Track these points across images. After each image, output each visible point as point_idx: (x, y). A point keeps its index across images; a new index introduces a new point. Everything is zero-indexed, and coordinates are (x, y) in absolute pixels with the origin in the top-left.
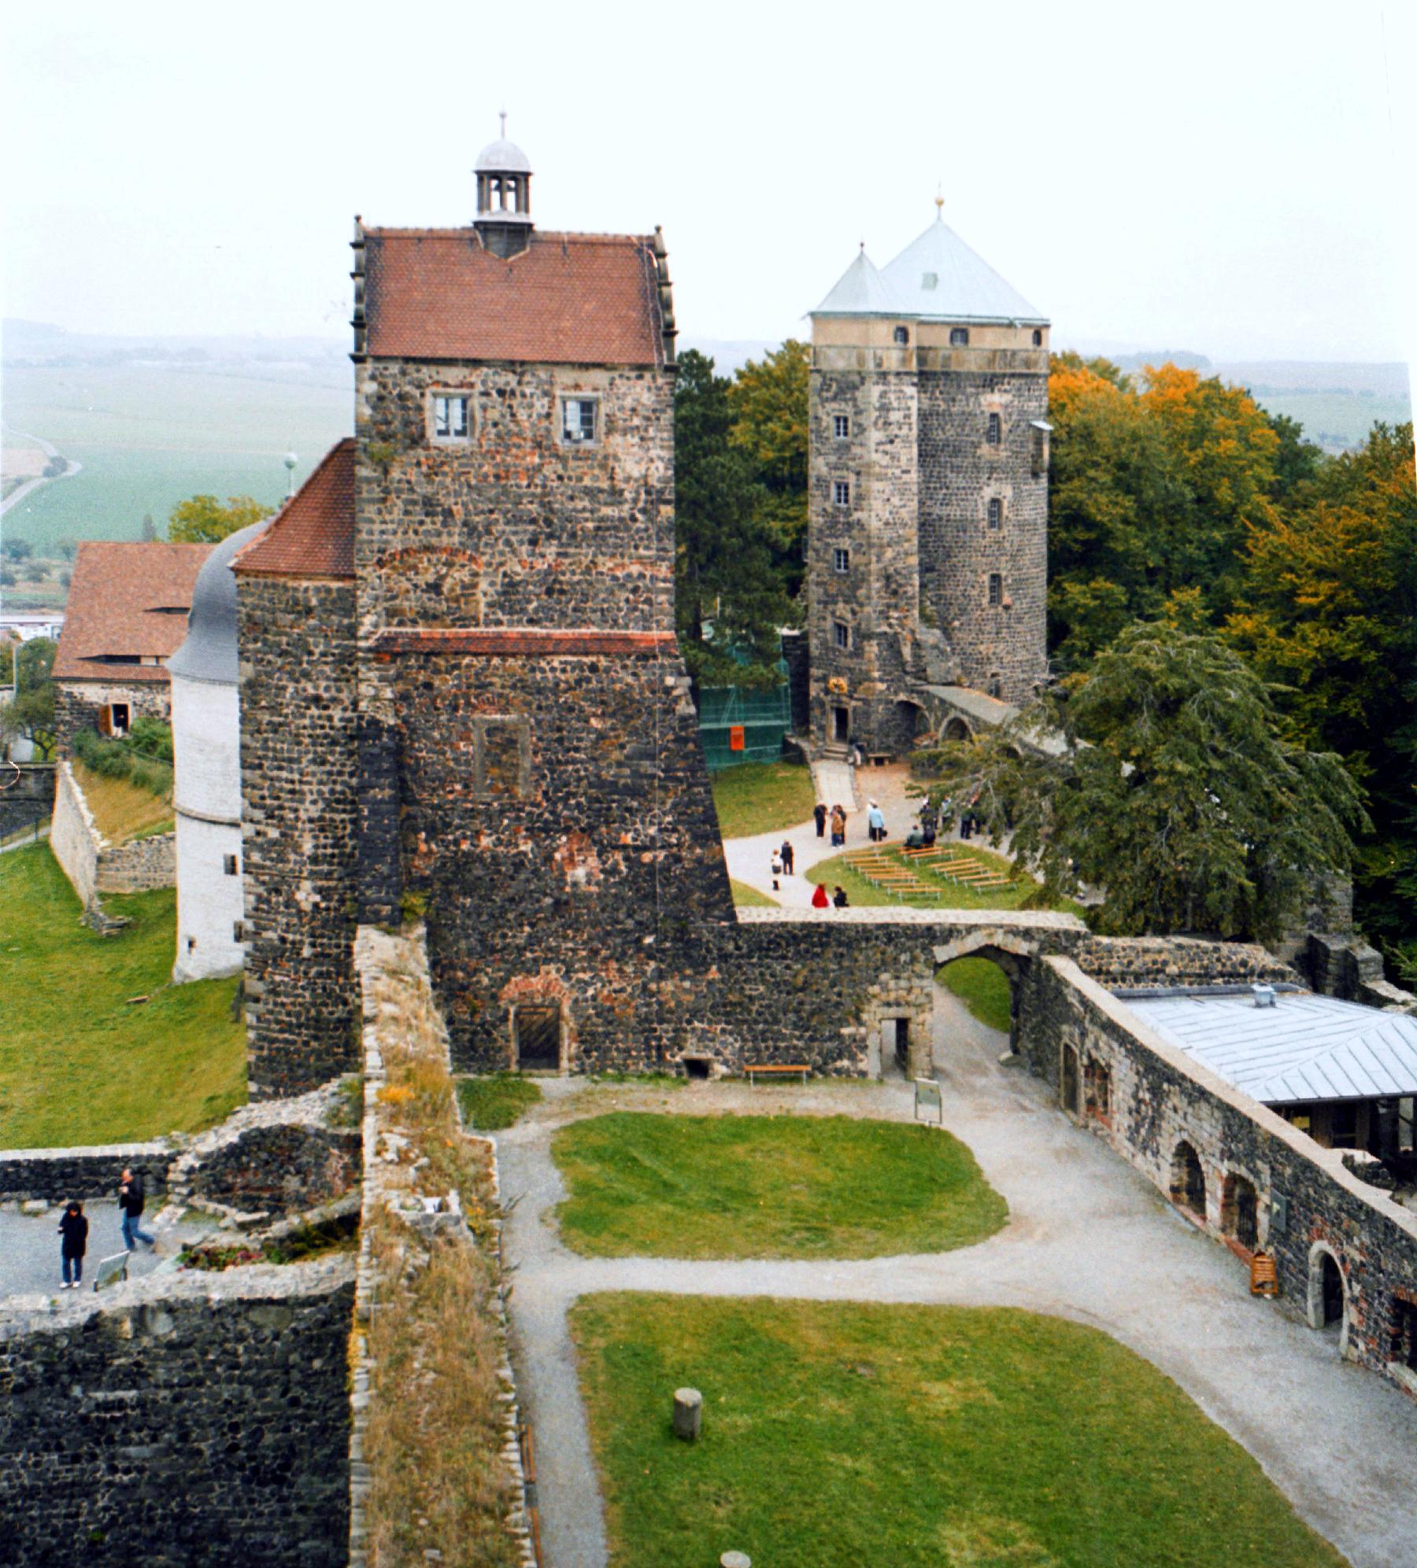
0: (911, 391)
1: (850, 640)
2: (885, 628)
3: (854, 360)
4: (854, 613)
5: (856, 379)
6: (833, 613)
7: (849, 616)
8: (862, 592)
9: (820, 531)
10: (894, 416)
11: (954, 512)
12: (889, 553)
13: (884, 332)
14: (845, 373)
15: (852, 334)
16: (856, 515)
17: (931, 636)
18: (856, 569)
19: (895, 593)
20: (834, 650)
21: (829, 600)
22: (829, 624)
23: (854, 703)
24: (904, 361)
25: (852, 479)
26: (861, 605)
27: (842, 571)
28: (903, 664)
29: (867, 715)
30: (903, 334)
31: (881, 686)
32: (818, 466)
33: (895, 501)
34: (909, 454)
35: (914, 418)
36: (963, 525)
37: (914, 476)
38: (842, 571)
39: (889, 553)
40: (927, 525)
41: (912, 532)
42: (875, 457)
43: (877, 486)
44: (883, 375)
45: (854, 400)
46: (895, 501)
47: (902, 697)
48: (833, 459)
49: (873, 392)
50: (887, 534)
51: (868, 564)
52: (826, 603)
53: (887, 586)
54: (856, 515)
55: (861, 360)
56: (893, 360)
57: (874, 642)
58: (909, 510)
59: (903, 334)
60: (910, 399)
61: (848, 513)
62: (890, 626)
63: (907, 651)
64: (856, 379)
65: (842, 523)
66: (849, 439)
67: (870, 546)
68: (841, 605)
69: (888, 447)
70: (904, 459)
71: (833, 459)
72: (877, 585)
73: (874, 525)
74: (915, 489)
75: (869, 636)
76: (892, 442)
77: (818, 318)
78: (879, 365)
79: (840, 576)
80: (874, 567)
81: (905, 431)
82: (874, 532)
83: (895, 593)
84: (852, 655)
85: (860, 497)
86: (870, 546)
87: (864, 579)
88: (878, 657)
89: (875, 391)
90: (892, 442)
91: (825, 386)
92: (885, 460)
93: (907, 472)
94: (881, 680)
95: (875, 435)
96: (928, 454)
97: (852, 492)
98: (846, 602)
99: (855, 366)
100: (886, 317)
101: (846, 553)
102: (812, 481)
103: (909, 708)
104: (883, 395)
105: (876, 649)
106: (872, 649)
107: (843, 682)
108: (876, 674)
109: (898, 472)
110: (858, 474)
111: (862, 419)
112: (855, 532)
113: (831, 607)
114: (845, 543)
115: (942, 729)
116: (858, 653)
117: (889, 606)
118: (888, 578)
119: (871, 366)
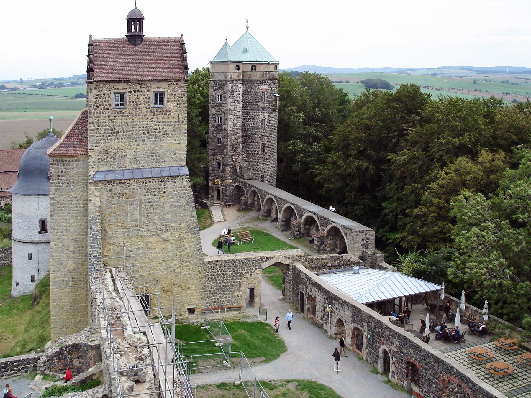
0: (240, 85)
1: (221, 167)
2: (232, 162)
3: (224, 76)
4: (223, 158)
5: (224, 82)
6: (216, 158)
9: (213, 132)
10: (236, 94)
11: (251, 124)
12: (233, 138)
13: (232, 67)
15: (223, 68)
16: (224, 126)
17: (245, 164)
19: (235, 151)
20: (216, 170)
21: (215, 155)
22: (215, 162)
23: (222, 187)
24: (238, 76)
25: (223, 115)
26: (225, 155)
27: (219, 144)
28: (237, 174)
29: (226, 190)
30: (238, 67)
32: (212, 111)
33: (235, 121)
34: (239, 106)
35: (241, 94)
36: (254, 128)
37: (241, 113)
38: (219, 144)
39: (233, 138)
40: (244, 128)
41: (240, 131)
42: (230, 107)
43: (230, 116)
45: (224, 89)
46: (235, 121)
47: (237, 184)
48: (217, 109)
49: (230, 86)
50: (233, 132)
51: (227, 142)
52: (214, 155)
53: (233, 149)
54: (224, 126)
55: (226, 77)
56: (235, 76)
57: (228, 167)
58: (239, 124)
59: (238, 67)
60: (240, 88)
61: (221, 126)
62: (233, 161)
63: (238, 169)
64: (224, 82)
65: (220, 129)
66: (222, 102)
67: (228, 136)
68: (219, 156)
70: (238, 107)
71: (217, 109)
72: (230, 148)
73: (229, 129)
74: (241, 117)
75: (227, 165)
76: (234, 102)
77: (212, 63)
78: (231, 78)
79: (218, 146)
80: (229, 143)
81: (238, 99)
82: (229, 131)
83: (235, 151)
85: (225, 120)
86: (228, 136)
87: (226, 147)
89: (230, 86)
90: (234, 102)
91: (215, 85)
94: (231, 179)
95: (230, 100)
96: (244, 106)
97: (222, 119)
98: (220, 155)
100: (234, 62)
101: (220, 139)
102: (210, 116)
104: (232, 87)
105: (229, 169)
106: (228, 169)
107: (219, 181)
108: (229, 177)
109: (236, 112)
110: (224, 113)
111: (225, 95)
114: (220, 136)
115: (249, 194)
116: (224, 171)
117: (233, 155)
118: (233, 146)
119: (229, 78)
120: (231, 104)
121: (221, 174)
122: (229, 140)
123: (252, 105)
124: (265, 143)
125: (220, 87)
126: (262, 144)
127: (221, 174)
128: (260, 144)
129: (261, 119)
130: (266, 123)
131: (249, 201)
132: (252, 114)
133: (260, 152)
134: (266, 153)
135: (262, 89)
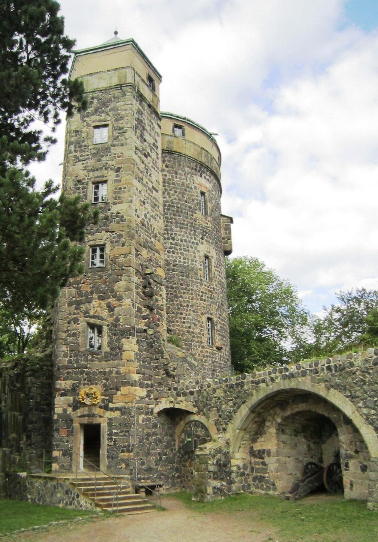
4: (111, 308)
6: (86, 313)
7: (105, 313)
8: (120, 286)
11: (179, 259)
14: (107, 90)
18: (114, 261)
19: (151, 296)
26: (120, 299)
31: (143, 392)
36: (187, 271)
44: (141, 98)
47: (164, 404)
48: (91, 163)
52: (78, 304)
57: (134, 340)
68: (95, 303)
69: (143, 158)
72: (136, 279)
75: (130, 332)
84: (108, 357)
88: (138, 357)
92: (142, 166)
93: (157, 191)
94: (141, 385)
98: (101, 298)
99: (115, 81)
103: (173, 415)
105: (136, 347)
107: (97, 389)
108: (136, 377)
112: (113, 226)
113: (83, 307)
116: (116, 351)
118: (145, 276)
120: (139, 154)
121: (105, 366)
122: (134, 251)
123: (178, 212)
124: (215, 319)
125: (105, 105)
126: (209, 319)
127: (105, 366)
128: (204, 319)
129: (202, 254)
130: (213, 269)
131: (239, 459)
132: (180, 234)
133: (204, 340)
134: (219, 349)
135: (200, 185)
